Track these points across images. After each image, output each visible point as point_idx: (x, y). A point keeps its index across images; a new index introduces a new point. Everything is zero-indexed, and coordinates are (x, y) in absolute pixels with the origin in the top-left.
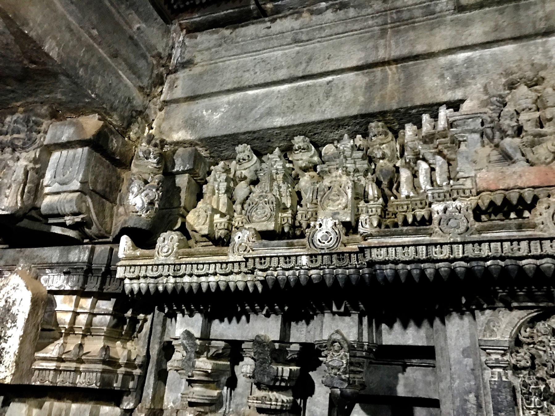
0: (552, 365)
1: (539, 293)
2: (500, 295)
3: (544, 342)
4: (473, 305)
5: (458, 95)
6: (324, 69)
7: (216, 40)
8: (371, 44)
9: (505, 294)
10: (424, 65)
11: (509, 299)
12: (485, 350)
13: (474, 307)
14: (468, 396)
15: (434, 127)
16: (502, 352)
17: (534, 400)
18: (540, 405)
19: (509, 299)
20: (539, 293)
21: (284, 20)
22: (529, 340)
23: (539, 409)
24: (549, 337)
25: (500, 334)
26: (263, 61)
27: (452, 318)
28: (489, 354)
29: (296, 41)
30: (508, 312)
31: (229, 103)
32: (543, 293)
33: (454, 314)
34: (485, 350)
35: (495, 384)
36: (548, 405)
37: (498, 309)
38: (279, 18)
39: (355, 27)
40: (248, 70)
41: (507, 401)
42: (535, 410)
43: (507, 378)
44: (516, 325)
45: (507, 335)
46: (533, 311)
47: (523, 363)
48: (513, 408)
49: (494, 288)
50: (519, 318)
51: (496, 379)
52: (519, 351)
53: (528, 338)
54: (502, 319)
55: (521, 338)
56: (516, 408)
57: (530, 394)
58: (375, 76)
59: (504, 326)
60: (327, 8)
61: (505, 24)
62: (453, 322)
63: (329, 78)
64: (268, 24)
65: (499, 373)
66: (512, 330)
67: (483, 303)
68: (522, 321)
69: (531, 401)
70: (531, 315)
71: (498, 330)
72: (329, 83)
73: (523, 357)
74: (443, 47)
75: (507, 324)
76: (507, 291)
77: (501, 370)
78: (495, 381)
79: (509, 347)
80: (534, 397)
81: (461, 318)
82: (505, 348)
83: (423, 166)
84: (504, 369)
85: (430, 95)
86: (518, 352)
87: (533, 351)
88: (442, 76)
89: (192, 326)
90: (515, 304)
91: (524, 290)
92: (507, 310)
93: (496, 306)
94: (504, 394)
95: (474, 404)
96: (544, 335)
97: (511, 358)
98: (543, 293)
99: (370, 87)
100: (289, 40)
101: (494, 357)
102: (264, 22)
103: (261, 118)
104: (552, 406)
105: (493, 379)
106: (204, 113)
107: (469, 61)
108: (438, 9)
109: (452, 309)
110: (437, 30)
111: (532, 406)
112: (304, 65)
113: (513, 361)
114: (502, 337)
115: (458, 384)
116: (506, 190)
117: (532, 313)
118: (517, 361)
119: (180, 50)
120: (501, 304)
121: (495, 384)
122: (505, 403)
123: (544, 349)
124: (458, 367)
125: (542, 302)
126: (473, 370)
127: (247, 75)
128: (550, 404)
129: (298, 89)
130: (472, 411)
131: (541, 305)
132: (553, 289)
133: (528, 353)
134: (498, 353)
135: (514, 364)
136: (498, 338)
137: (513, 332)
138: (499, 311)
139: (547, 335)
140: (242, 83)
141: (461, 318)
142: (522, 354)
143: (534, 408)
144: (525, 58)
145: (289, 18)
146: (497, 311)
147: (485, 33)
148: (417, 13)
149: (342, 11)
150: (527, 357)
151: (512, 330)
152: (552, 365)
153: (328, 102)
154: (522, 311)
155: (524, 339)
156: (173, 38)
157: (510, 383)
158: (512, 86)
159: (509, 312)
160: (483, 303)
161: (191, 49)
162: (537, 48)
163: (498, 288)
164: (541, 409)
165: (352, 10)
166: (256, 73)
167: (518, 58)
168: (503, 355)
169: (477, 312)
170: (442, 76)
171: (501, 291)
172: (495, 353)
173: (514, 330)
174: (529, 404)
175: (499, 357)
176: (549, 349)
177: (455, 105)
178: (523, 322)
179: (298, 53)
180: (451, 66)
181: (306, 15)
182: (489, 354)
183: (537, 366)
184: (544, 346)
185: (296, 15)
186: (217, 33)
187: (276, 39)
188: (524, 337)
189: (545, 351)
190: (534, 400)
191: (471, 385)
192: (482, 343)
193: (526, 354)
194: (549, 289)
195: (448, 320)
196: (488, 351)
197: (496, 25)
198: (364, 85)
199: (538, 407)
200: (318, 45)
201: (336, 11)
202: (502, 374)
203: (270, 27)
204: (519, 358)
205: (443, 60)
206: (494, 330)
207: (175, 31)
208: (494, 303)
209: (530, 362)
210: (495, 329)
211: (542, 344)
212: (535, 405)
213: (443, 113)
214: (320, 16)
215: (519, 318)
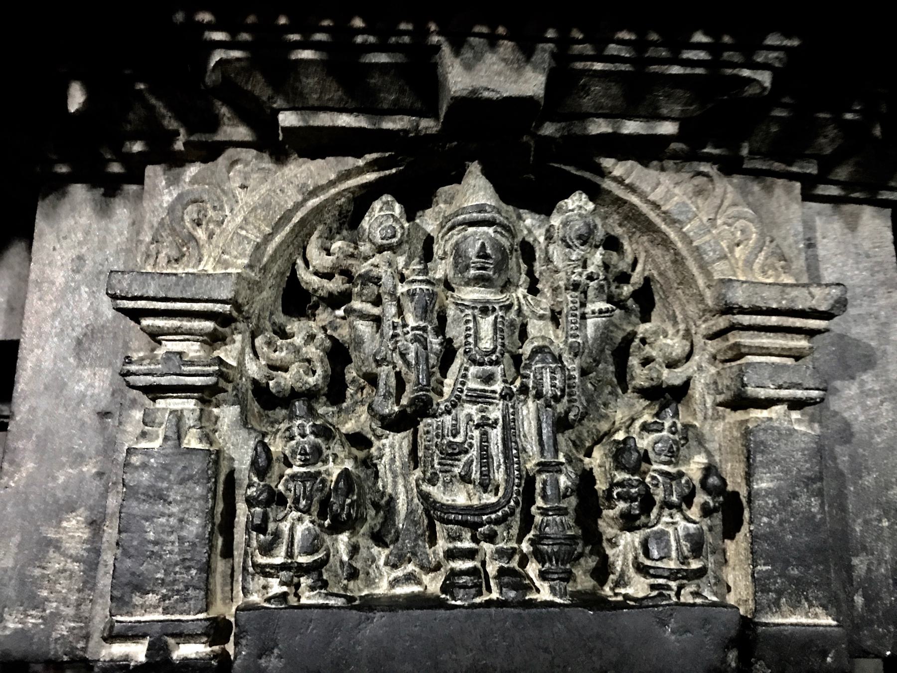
0: (398, 375)
1: (383, 58)
2: (217, 56)
3: (377, 281)
4: (134, 138)
9: (236, 54)
11: (259, 88)
12: (136, 315)
13: (137, 147)
14: (58, 525)
16: (209, 325)
17: (292, 529)
18: (311, 550)
19: (259, 88)
20: (383, 58)
22: (336, 285)
23: (302, 570)
24: (401, 261)
25: (216, 252)
27: (65, 206)
28: (155, 336)
30: (267, 163)
32: (399, 58)
33: (79, 192)
34: (136, 315)
35: (144, 466)
36: (354, 550)
37: (231, 152)
41: (181, 539)
42: (284, 575)
43: (207, 437)
44: (286, 217)
45: (242, 255)
46: (361, 162)
47: (286, 380)
48: (207, 569)
49: (190, 16)
50: (301, 188)
51: (156, 444)
52: (288, 328)
53: (329, 276)
54: (241, 194)
55: (306, 276)
56: (220, 565)
57: (276, 499)
59: (239, 219)
62: (67, 223)
65: (178, 416)
66: (268, 238)
67: (171, 123)
68: (313, 202)
69: (277, 535)
70: (353, 182)
71: (211, 236)
73: (297, 350)
75: (254, 209)
76: (245, 37)
77: (188, 405)
78: (147, 452)
79: (233, 302)
80: (295, 514)
81: (103, 211)
82: (218, 307)
84: (202, 400)
86: (283, 334)
87: (343, 333)
90: (288, 119)
91: (319, 37)
92: (266, 156)
93: (220, 137)
94: (175, 509)
95: (76, 559)
96: (381, 249)
97: (249, 356)
98: (399, 58)
101: (171, 346)
104: (375, 550)
105: (144, 444)
109: (63, 169)
111: (279, 559)
113: (254, 369)
114: (219, 262)
115: (30, 475)
117: (360, 171)
118: (273, 367)
120: (242, 133)
121: (144, 466)
122: (172, 551)
123: (376, 311)
124: (44, 403)
125: (396, 110)
126: (104, 414)
128: (364, 542)
130: (62, 587)
131: (390, 124)
132: (435, 39)
133: (321, 336)
134: (190, 332)
135: (254, 382)
136: (208, 266)
137: (270, 249)
138: (234, 163)
139: (390, 248)
141: (103, 211)
142: (298, 340)
143: (283, 567)
146: (222, 161)
150: (312, 351)
151: (268, 238)
152: (398, 375)
154: (320, 162)
155: (316, 281)
157: (216, 457)
159: (271, 166)
160: (171, 123)
163: (205, 17)
164: (315, 568)
168: (214, 340)
169: (154, 174)
171: (219, 36)
172: (176, 332)
173: (278, 239)
174: (267, 549)
175: (193, 349)
176: (393, 310)
178: (318, 210)
182: (155, 336)
183: (350, 390)
184: (377, 301)
188: (316, 273)
189: (377, 320)
190: (292, 529)
191: (81, 478)
192: (123, 285)
193: (311, 337)
194: (421, 33)
195: (47, 216)
196: (146, 322)
199: (304, 559)
202: (190, 420)
204: (281, 355)
206: (192, 238)
208: (215, 124)
209: (319, 371)
210: (201, 234)
211: (372, 289)
212: (290, 554)
215: (301, 188)
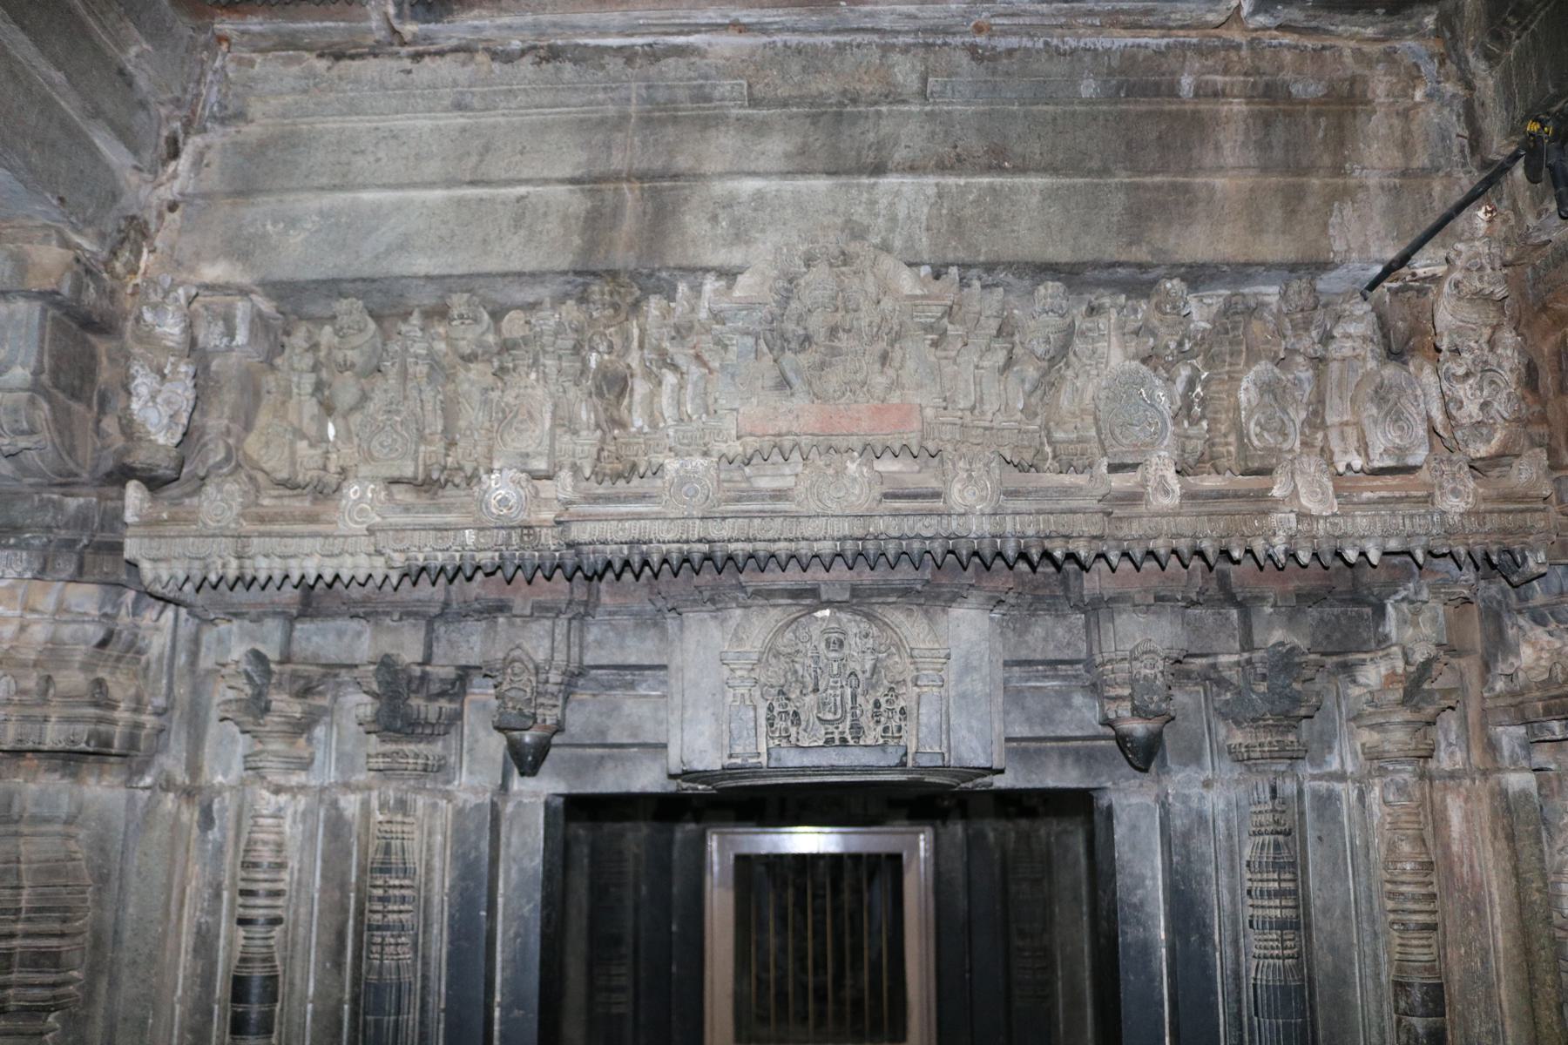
5: (735, 257)
6: (512, 174)
7: (297, 78)
8: (599, 137)
10: (687, 192)
15: (693, 310)
21: (439, 61)
26: (395, 137)
29: (459, 106)
31: (321, 213)
38: (430, 54)
39: (573, 101)
40: (363, 152)
58: (603, 200)
60: (523, 53)
61: (818, 144)
63: (522, 190)
64: (407, 64)
72: (520, 199)
74: (720, 168)
83: (670, 378)
85: (691, 252)
88: (714, 219)
89: (264, 642)
99: (594, 220)
100: (447, 102)
102: (396, 55)
103: (388, 252)
106: (269, 227)
107: (759, 196)
108: (717, 94)
110: (712, 133)
112: (474, 159)
116: (779, 435)
119: (215, 88)
127: (360, 161)
129: (460, 202)
140: (351, 177)
144: (841, 208)
145: (449, 58)
147: (787, 156)
148: (682, 94)
149: (550, 66)
153: (516, 239)
156: (202, 62)
158: (809, 261)
161: (240, 90)
162: (861, 193)
165: (568, 66)
166: (378, 160)
167: (831, 206)
170: (714, 219)
177: (729, 275)
179: (464, 130)
180: (729, 203)
181: (481, 58)
185: (462, 56)
186: (299, 61)
187: (422, 96)
197: (805, 144)
198: (583, 214)
200: (502, 120)
201: (539, 63)
203: (409, 72)
205: (719, 188)
207: (206, 46)
213: (710, 284)
214: (507, 67)
